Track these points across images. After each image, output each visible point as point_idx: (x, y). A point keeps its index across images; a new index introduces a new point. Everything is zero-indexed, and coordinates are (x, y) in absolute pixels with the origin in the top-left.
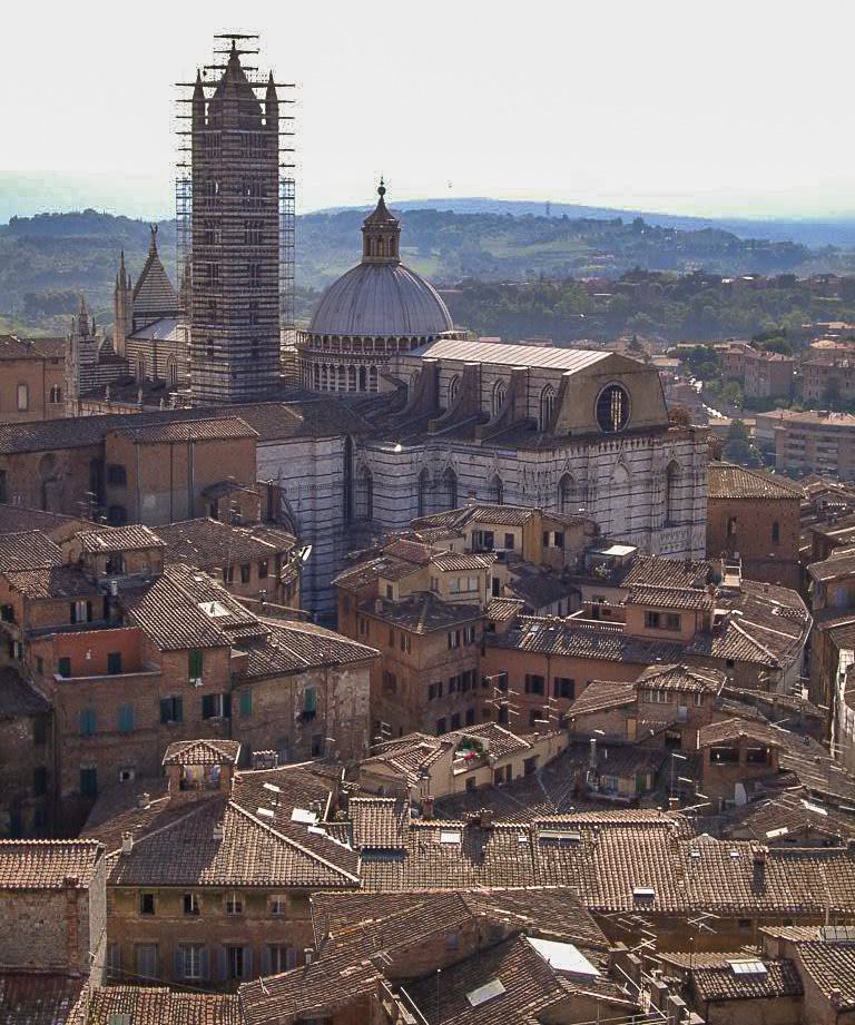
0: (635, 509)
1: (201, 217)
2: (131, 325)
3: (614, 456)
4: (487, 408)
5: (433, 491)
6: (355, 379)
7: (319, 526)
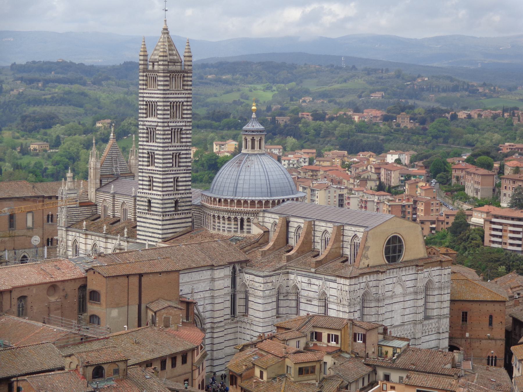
0: (407, 310)
1: (145, 125)
2: (99, 182)
4: (318, 247)
5: (285, 298)
6: (237, 225)
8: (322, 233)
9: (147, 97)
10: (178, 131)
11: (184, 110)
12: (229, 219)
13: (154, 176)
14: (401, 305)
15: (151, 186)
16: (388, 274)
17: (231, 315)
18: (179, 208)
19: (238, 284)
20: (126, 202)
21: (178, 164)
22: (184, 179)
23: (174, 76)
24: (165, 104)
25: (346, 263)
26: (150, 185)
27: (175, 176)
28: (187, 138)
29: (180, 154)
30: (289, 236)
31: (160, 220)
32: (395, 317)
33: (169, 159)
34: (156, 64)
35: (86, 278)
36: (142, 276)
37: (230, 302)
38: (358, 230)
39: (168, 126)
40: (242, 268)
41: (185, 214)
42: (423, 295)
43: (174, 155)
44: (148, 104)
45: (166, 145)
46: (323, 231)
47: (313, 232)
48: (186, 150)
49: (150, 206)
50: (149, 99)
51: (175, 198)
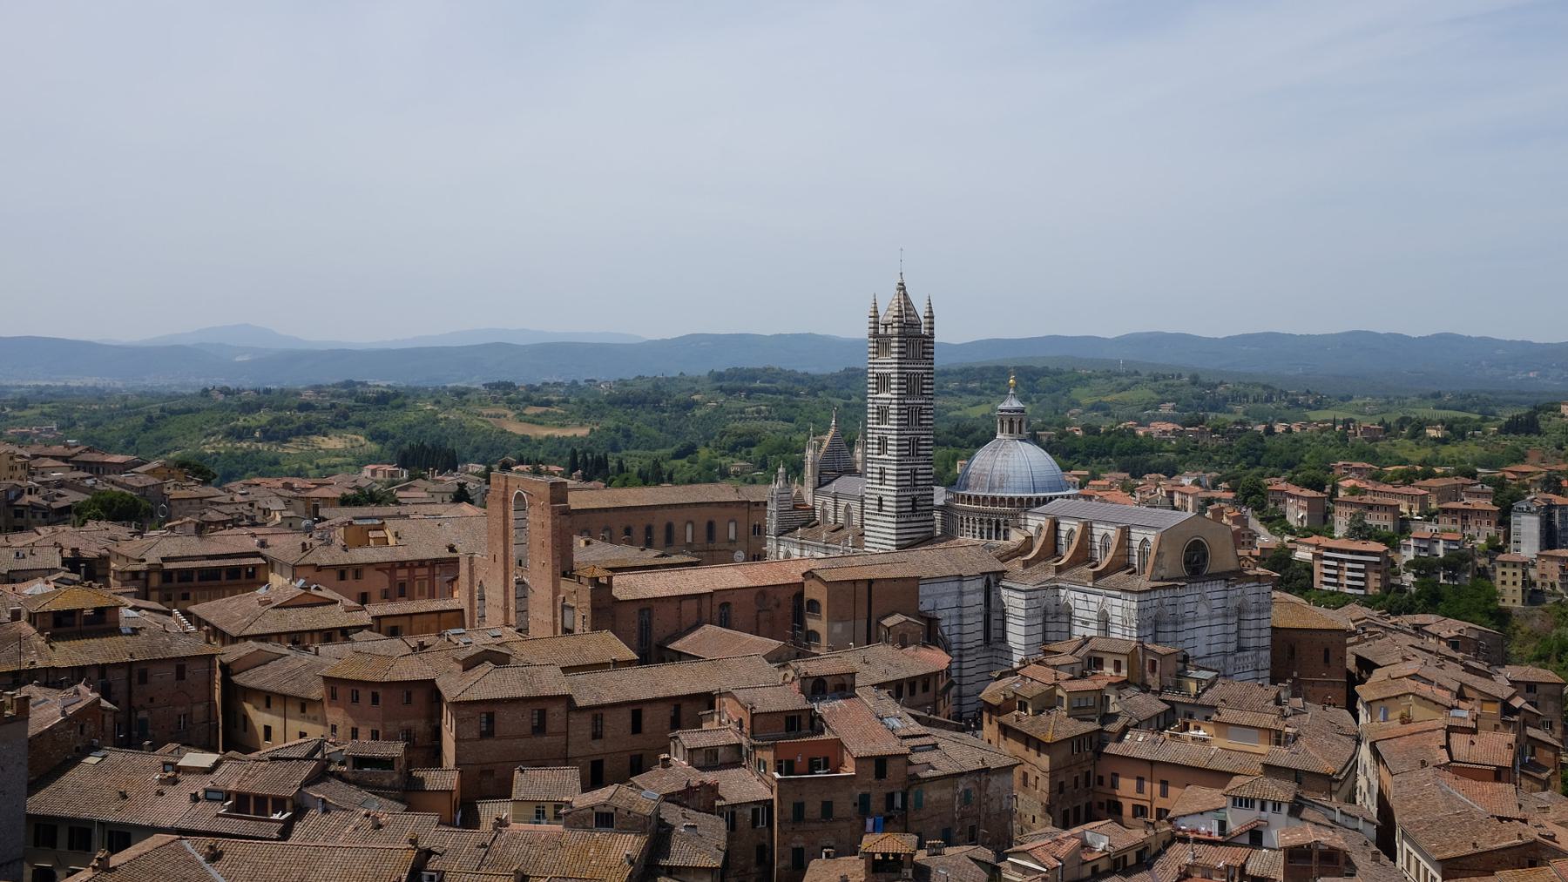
0: (1214, 638)
3: (1197, 596)
7: (965, 646)
13: (886, 466)
15: (882, 480)
26: (881, 479)
28: (927, 419)
33: (906, 445)
35: (803, 583)
39: (904, 404)
40: (999, 580)
42: (1235, 619)
46: (1102, 534)
49: (880, 505)
50: (880, 371)
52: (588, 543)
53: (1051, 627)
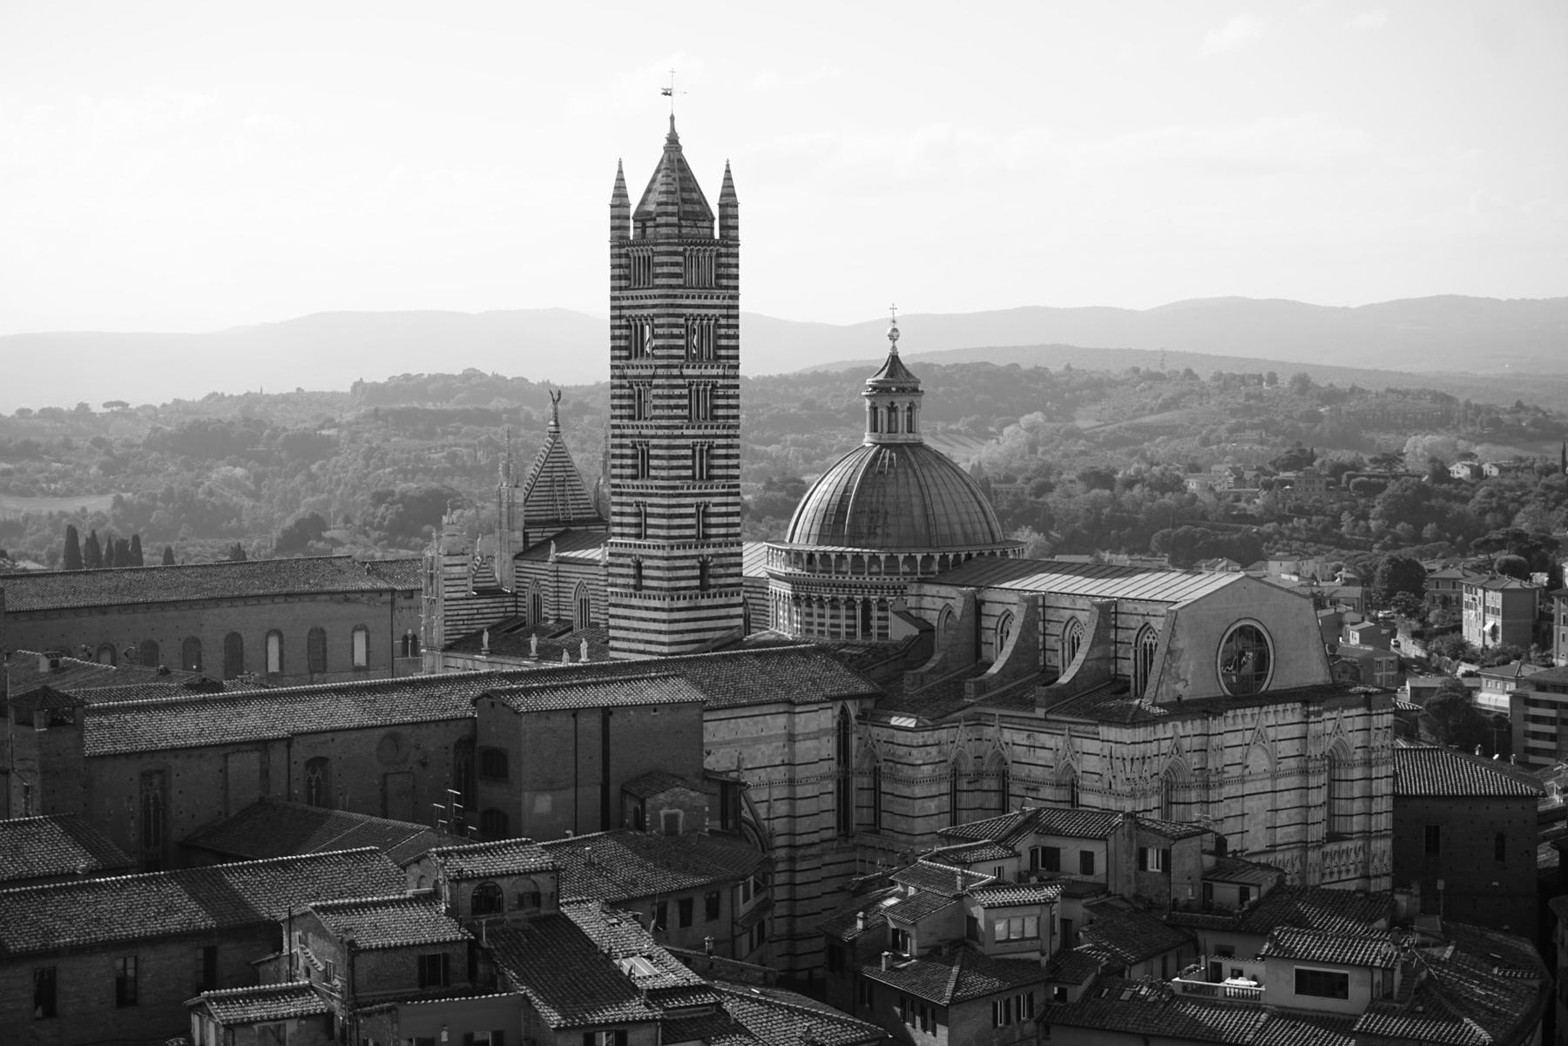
2: (521, 539)
3: (1248, 733)
5: (977, 786)
6: (854, 617)
7: (800, 841)
8: (1063, 626)
9: (629, 307)
10: (705, 390)
11: (720, 337)
12: (835, 603)
13: (649, 500)
14: (1266, 801)
16: (1230, 721)
17: (839, 830)
18: (712, 581)
19: (854, 753)
20: (585, 582)
21: (707, 471)
22: (723, 509)
23: (695, 253)
24: (673, 320)
25: (1127, 695)
27: (699, 500)
29: (710, 447)
30: (983, 640)
31: (663, 610)
32: (1252, 831)
33: (685, 457)
34: (650, 224)
36: (611, 713)
37: (835, 795)
38: (1154, 610)
39: (682, 376)
41: (726, 596)
42: (1323, 779)
43: (698, 448)
44: (632, 323)
45: (677, 422)
47: (1041, 624)
48: (727, 436)
51: (699, 556)
52: (54, 664)
53: (965, 799)
